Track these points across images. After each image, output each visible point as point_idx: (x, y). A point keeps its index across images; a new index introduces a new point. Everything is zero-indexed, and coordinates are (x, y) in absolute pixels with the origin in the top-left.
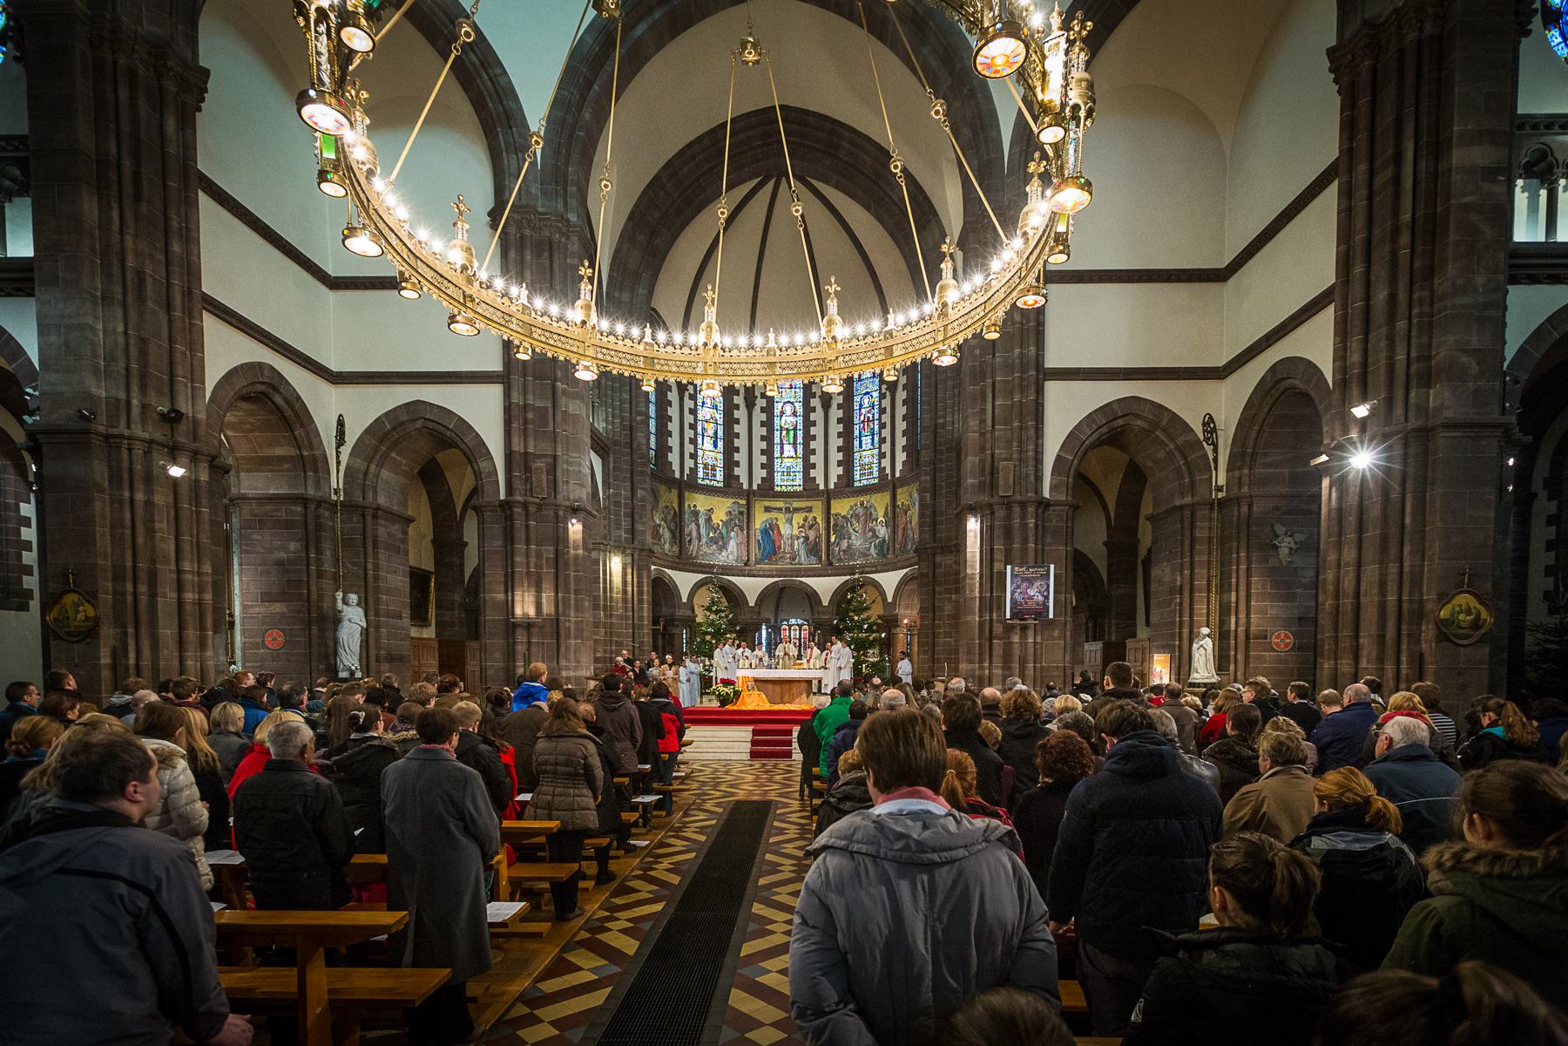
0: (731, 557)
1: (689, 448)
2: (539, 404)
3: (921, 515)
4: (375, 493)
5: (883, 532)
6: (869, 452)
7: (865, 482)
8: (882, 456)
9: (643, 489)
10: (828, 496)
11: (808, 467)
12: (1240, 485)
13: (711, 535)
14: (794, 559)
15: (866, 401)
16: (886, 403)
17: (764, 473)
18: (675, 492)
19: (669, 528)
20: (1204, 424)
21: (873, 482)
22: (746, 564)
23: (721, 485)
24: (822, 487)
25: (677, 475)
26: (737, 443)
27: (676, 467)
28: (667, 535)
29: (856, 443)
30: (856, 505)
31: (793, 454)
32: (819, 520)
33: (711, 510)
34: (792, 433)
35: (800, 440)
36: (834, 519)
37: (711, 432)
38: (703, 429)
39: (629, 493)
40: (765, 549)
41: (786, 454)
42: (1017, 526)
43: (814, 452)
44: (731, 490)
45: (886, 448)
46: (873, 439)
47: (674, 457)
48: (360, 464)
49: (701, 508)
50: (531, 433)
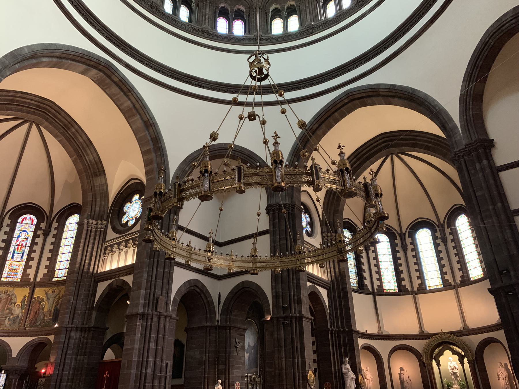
5: (18, 311)
7: (10, 280)
8: (27, 267)
12: (226, 322)
15: (23, 235)
16: (39, 240)
21: (16, 280)
29: (10, 256)
42: (162, 326)
46: (22, 256)
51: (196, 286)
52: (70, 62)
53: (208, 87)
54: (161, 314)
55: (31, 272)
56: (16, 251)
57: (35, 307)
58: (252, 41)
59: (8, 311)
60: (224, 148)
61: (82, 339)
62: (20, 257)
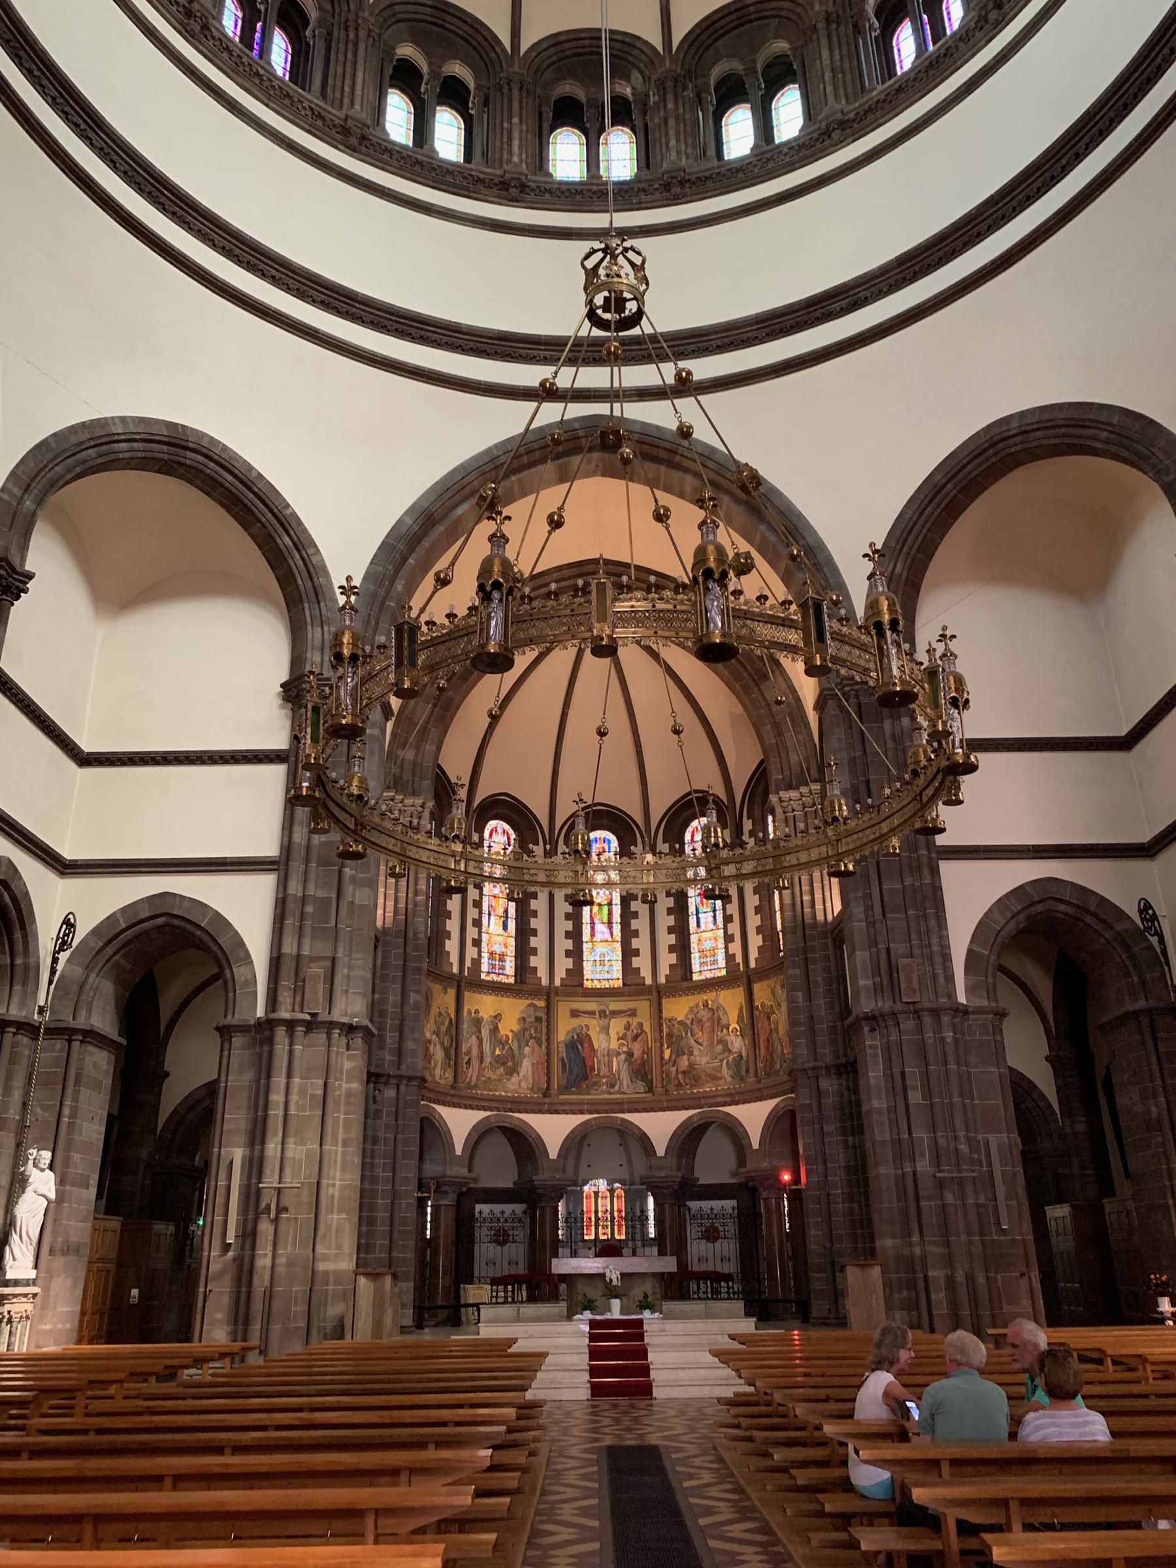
0: (524, 1085)
1: (471, 932)
2: (321, 894)
3: (793, 1023)
4: (90, 1011)
5: (738, 1044)
6: (710, 934)
7: (709, 975)
8: (729, 939)
9: (418, 992)
10: (658, 994)
11: (628, 953)
13: (498, 1052)
14: (613, 1086)
17: (569, 963)
18: (452, 992)
19: (442, 1044)
20: (1140, 911)
21: (719, 974)
22: (545, 1095)
23: (512, 980)
24: (649, 981)
25: (455, 970)
26: (534, 923)
27: (454, 959)
28: (438, 1054)
30: (697, 1006)
31: (607, 936)
32: (647, 1028)
33: (498, 1017)
34: (605, 909)
35: (617, 917)
36: (669, 1027)
37: (500, 911)
38: (490, 906)
39: (399, 998)
40: (571, 1071)
41: (598, 937)
43: (636, 934)
44: (525, 987)
45: (734, 928)
47: (452, 946)
48: (78, 971)
49: (486, 1014)
50: (308, 930)
51: (1050, 898)
52: (513, 478)
53: (880, 291)
54: (919, 1006)
55: (736, 948)
56: (701, 909)
57: (762, 1027)
58: (978, 34)
59: (720, 1047)
60: (986, 445)
61: (846, 1093)
62: (711, 919)
